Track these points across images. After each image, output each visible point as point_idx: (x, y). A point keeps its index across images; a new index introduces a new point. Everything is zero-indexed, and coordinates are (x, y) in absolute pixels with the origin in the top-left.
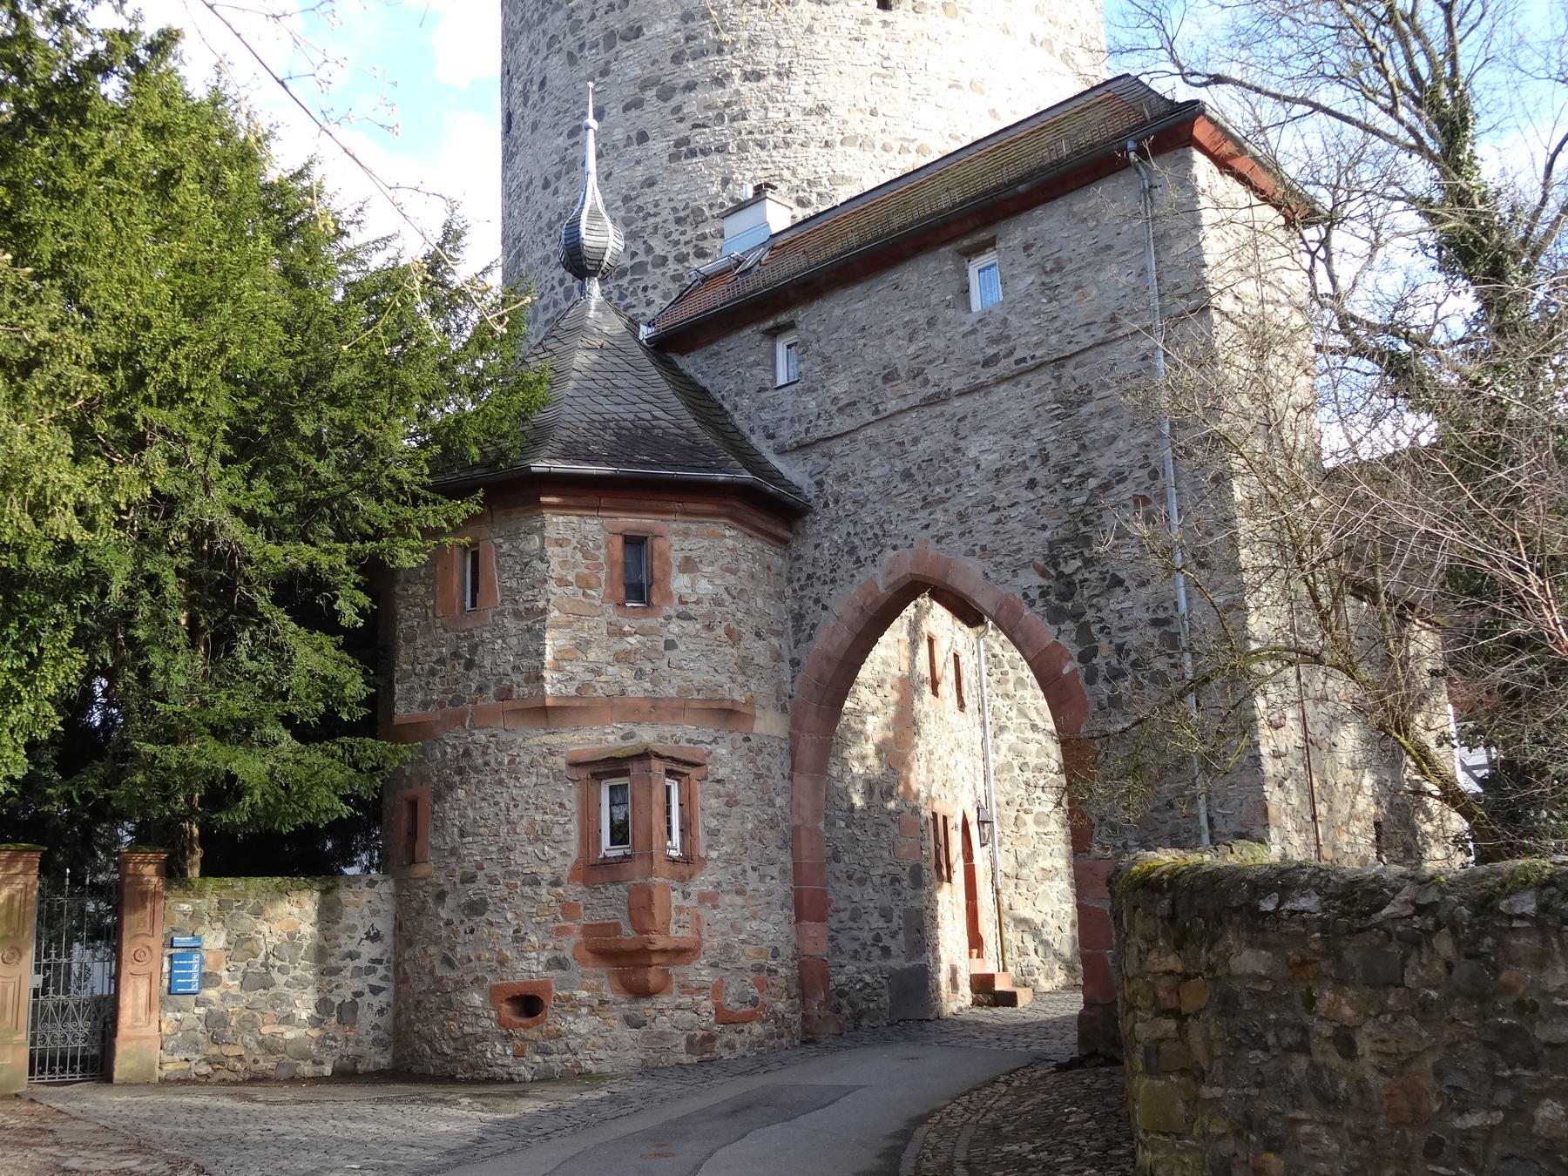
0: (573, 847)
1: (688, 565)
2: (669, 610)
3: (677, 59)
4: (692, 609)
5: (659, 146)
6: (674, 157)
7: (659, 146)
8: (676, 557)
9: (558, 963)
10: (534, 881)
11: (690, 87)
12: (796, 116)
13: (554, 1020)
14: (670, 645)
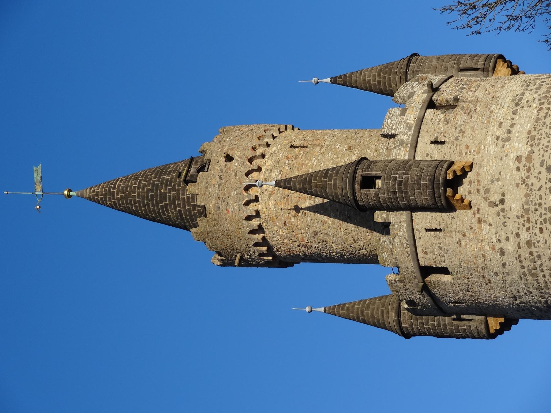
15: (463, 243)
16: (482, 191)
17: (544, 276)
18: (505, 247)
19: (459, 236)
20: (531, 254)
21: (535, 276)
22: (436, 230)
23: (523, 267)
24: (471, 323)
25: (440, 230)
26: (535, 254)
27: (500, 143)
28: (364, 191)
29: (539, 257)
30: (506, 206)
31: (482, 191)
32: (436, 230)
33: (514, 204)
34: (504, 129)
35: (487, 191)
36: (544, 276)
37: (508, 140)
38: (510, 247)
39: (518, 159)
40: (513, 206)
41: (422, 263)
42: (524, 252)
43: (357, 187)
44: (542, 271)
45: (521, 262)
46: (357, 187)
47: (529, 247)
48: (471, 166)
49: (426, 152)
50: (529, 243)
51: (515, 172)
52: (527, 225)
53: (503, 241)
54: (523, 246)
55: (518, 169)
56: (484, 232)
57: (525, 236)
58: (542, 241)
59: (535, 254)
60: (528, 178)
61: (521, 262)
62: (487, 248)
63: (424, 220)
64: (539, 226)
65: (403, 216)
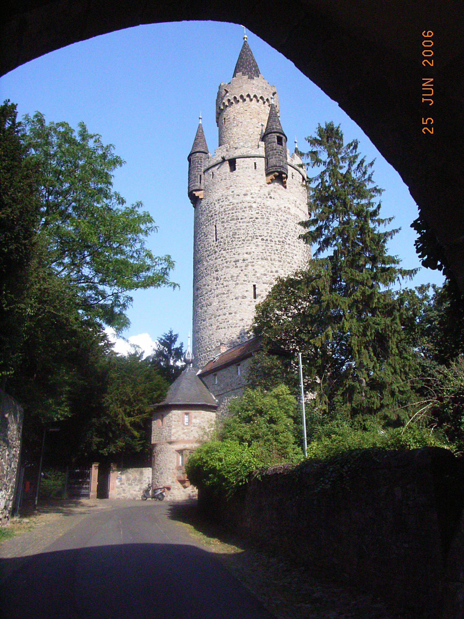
0: (175, 464)
1: (195, 417)
2: (192, 425)
3: (217, 310)
4: (196, 425)
5: (214, 327)
6: (216, 329)
7: (214, 327)
8: (193, 416)
9: (173, 482)
10: (169, 469)
11: (219, 316)
12: (238, 321)
13: (172, 490)
14: (192, 431)
15: (249, 178)
16: (275, 190)
17: (233, 213)
18: (248, 196)
19: (253, 177)
20: (245, 208)
21: (233, 209)
22: (255, 167)
23: (237, 204)
24: (199, 183)
25: (255, 169)
26: (245, 209)
27: (294, 202)
28: (276, 137)
29: (244, 211)
30: (269, 199)
31: (275, 190)
32: (255, 167)
33: (269, 202)
34: (299, 206)
35: (275, 192)
36: (233, 213)
37: (295, 206)
38: (248, 198)
39: (289, 208)
40: (269, 202)
41: (237, 160)
42: (246, 204)
43: (278, 135)
44: (236, 212)
45: (241, 203)
46: (278, 135)
47: (249, 207)
48: (285, 187)
49: (290, 170)
50: (251, 207)
51: (284, 205)
52: (260, 207)
53: (251, 196)
54: (249, 204)
55: (285, 207)
56: (255, 188)
57: (254, 205)
58: (252, 213)
59: (245, 209)
60: (282, 211)
61: (241, 203)
62: (248, 188)
63: (261, 163)
64: (260, 212)
65: (263, 154)
